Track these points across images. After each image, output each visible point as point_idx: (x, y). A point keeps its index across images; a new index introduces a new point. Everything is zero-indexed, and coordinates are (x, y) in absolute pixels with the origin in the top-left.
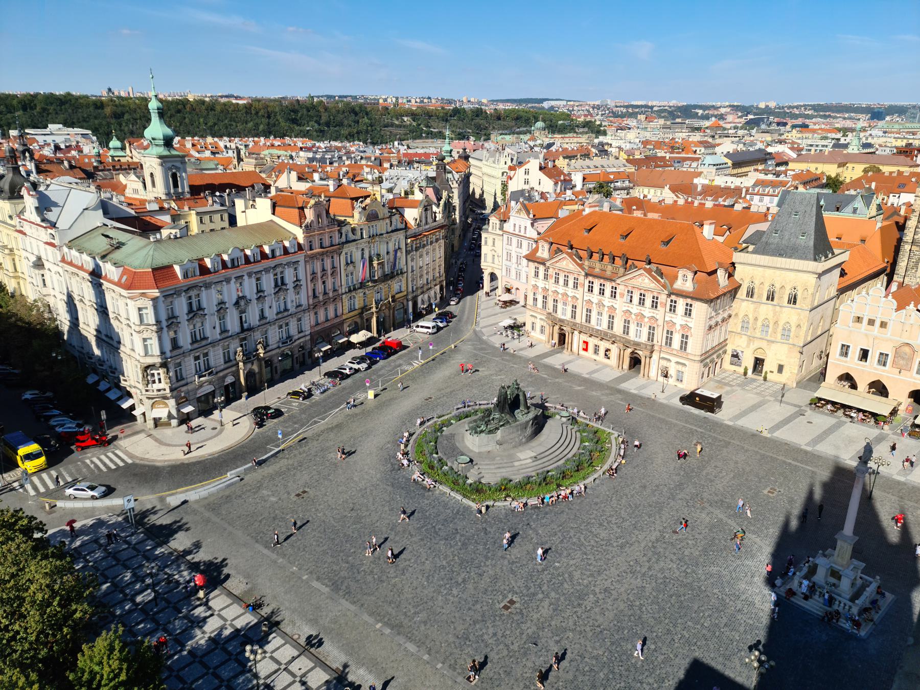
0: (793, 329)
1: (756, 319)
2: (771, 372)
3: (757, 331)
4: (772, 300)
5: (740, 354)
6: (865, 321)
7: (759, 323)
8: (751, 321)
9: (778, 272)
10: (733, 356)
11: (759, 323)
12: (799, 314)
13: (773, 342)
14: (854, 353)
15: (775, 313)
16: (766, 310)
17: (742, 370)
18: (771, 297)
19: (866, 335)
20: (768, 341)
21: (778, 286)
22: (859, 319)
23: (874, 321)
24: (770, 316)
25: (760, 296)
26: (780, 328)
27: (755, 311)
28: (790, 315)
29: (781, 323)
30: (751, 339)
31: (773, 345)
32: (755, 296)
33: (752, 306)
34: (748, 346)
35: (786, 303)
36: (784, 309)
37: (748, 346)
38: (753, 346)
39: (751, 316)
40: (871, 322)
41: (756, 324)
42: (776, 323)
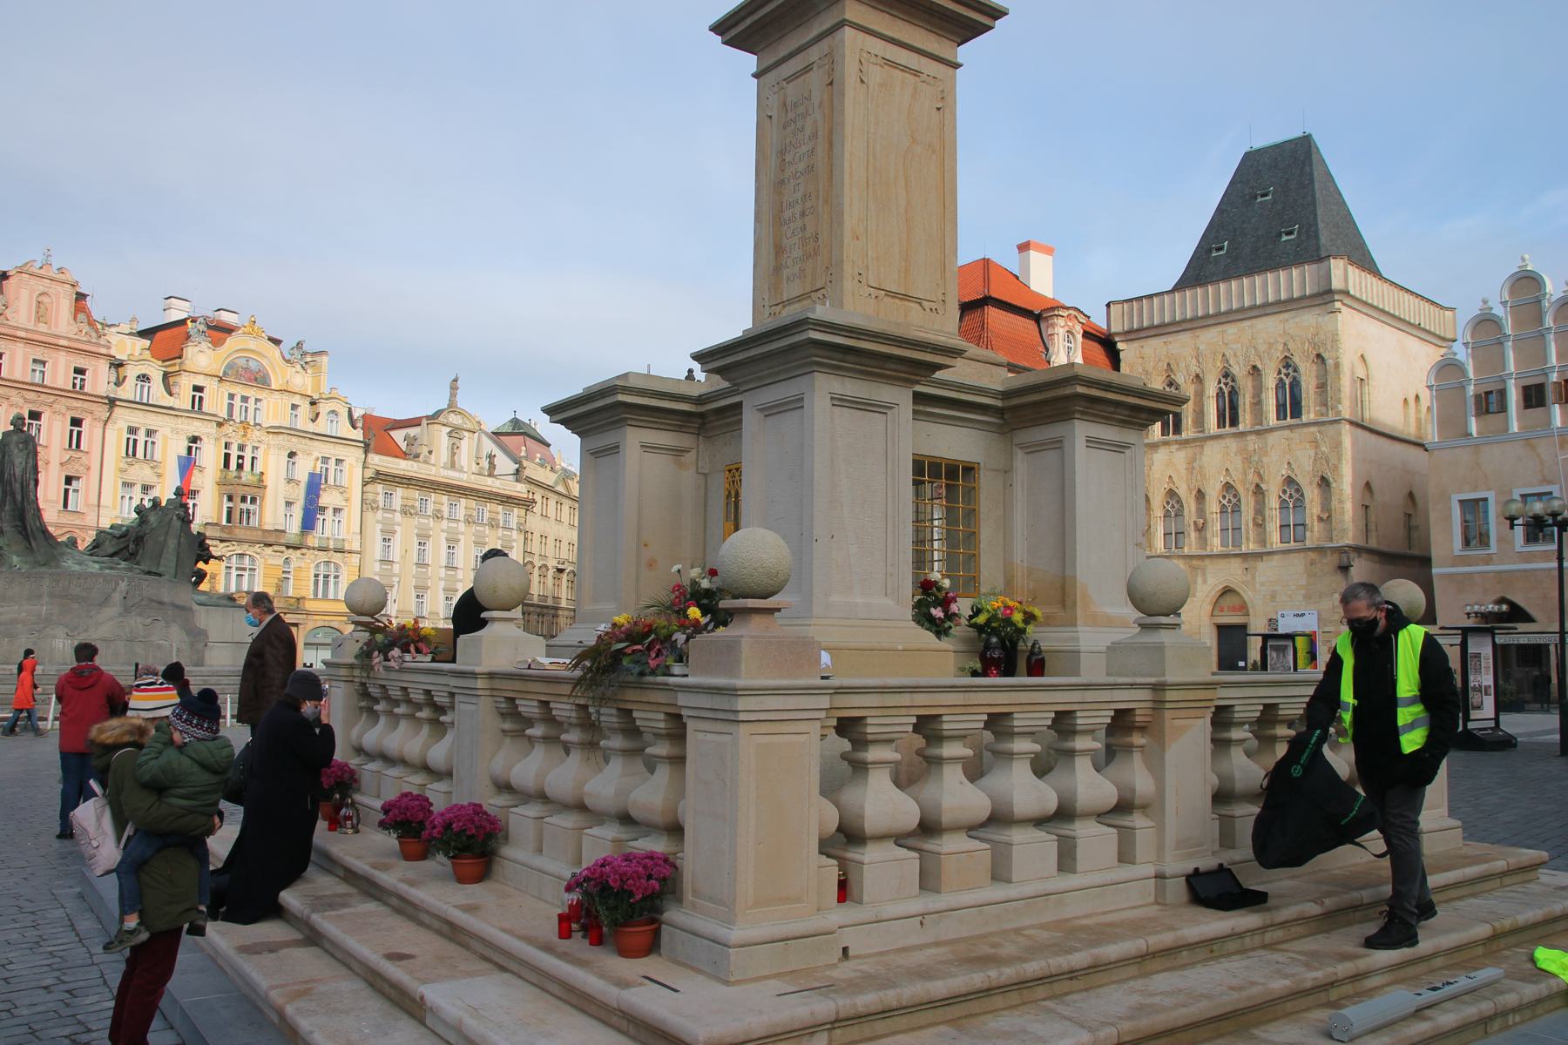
1: (1200, 495)
4: (1234, 422)
7: (1213, 507)
8: (1190, 506)
9: (1232, 330)
11: (1213, 507)
12: (1315, 444)
13: (1258, 556)
15: (1247, 460)
18: (1229, 414)
20: (1245, 556)
23: (1540, 388)
24: (1236, 479)
26: (1273, 502)
27: (1191, 469)
28: (1286, 454)
33: (1180, 457)
35: (1272, 419)
36: (1272, 438)
39: (1182, 491)
41: (1201, 512)
42: (1259, 491)
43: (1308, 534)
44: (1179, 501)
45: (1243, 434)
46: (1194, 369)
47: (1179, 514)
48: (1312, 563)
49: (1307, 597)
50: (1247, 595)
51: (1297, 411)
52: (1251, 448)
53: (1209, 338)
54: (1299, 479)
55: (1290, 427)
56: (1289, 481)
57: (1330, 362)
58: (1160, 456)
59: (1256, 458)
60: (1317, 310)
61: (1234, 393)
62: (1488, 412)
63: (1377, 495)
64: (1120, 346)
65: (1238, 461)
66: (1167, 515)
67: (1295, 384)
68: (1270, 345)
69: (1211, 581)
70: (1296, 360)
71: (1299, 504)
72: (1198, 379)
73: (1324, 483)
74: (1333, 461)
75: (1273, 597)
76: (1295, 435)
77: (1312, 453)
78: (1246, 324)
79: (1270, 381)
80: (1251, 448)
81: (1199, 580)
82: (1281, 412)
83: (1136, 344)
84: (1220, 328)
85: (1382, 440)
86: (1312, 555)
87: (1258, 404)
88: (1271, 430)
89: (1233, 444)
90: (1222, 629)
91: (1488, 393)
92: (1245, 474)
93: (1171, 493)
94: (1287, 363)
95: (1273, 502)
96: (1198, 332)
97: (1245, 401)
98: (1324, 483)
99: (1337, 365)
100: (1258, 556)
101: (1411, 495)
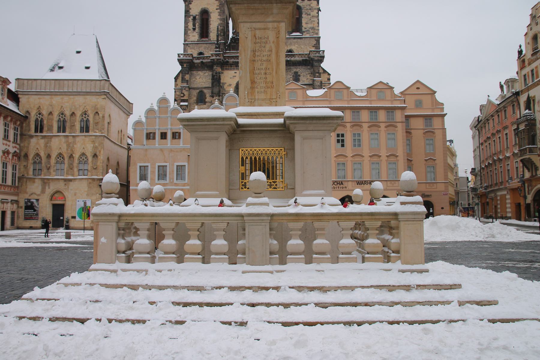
0: (90, 159)
1: (49, 156)
2: (74, 217)
3: (52, 171)
5: (36, 203)
6: (158, 136)
7: (53, 161)
9: (66, 98)
10: (27, 208)
12: (93, 142)
14: (153, 172)
15: (68, 146)
16: (58, 144)
17: (39, 223)
18: (62, 128)
19: (161, 150)
20: (65, 180)
21: (68, 113)
22: (150, 136)
24: (64, 150)
25: (50, 129)
26: (76, 161)
27: (46, 146)
29: (76, 156)
30: (45, 182)
31: (71, 183)
32: (45, 128)
33: (42, 142)
34: (43, 191)
36: (78, 139)
37: (43, 191)
38: (49, 191)
39: (42, 154)
40: (164, 136)
42: (71, 157)
43: (89, 173)
44: (40, 158)
45: (67, 136)
46: (50, 110)
47: (40, 163)
48: (90, 183)
49: (88, 195)
50: (66, 194)
51: (87, 131)
52: (70, 141)
53: (56, 100)
54: (87, 154)
55: (85, 136)
56: (83, 154)
57: (101, 115)
58: (33, 141)
59: (71, 145)
60: (98, 97)
61: (64, 121)
62: (150, 139)
63: (110, 162)
64: (19, 96)
65: (64, 146)
66: (35, 163)
67: (87, 121)
68: (80, 106)
69: (52, 188)
70: (89, 112)
71: (86, 163)
72: (51, 113)
73: (95, 156)
74: (100, 149)
75: (75, 194)
76: (87, 139)
77: (92, 145)
78: (72, 97)
79: (78, 118)
80: (70, 141)
81: (47, 187)
82: (82, 130)
83: (27, 96)
84: (62, 96)
85: (112, 144)
86: (90, 181)
87: (73, 126)
88: (78, 136)
89: (63, 140)
90: (55, 206)
91: (150, 133)
92: (67, 150)
93: (38, 155)
94: (85, 113)
95: (76, 161)
96: (53, 96)
97: (68, 125)
98: (95, 156)
99: (103, 117)
100: (70, 180)
101: (118, 163)
